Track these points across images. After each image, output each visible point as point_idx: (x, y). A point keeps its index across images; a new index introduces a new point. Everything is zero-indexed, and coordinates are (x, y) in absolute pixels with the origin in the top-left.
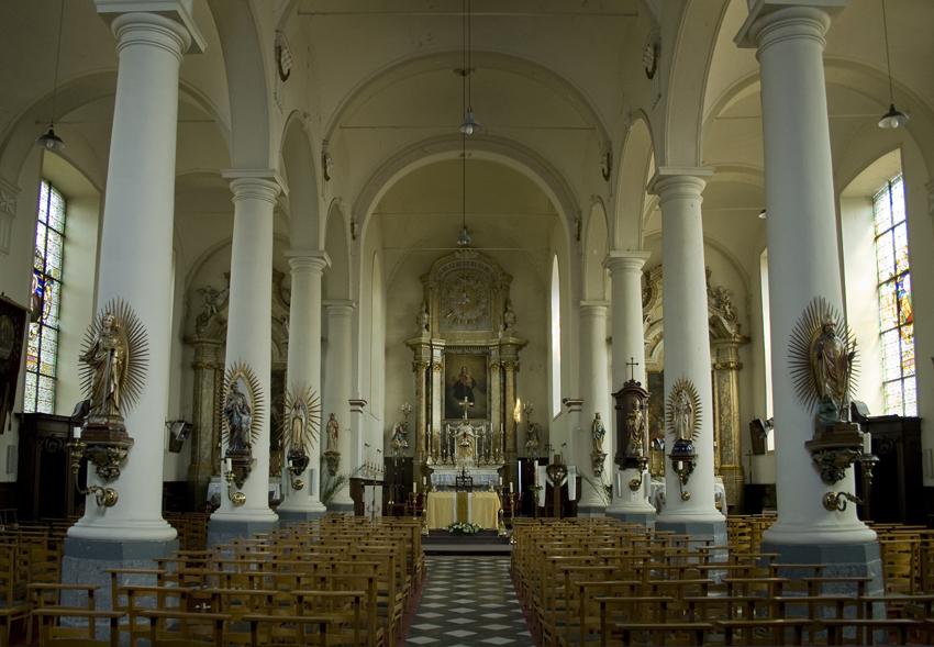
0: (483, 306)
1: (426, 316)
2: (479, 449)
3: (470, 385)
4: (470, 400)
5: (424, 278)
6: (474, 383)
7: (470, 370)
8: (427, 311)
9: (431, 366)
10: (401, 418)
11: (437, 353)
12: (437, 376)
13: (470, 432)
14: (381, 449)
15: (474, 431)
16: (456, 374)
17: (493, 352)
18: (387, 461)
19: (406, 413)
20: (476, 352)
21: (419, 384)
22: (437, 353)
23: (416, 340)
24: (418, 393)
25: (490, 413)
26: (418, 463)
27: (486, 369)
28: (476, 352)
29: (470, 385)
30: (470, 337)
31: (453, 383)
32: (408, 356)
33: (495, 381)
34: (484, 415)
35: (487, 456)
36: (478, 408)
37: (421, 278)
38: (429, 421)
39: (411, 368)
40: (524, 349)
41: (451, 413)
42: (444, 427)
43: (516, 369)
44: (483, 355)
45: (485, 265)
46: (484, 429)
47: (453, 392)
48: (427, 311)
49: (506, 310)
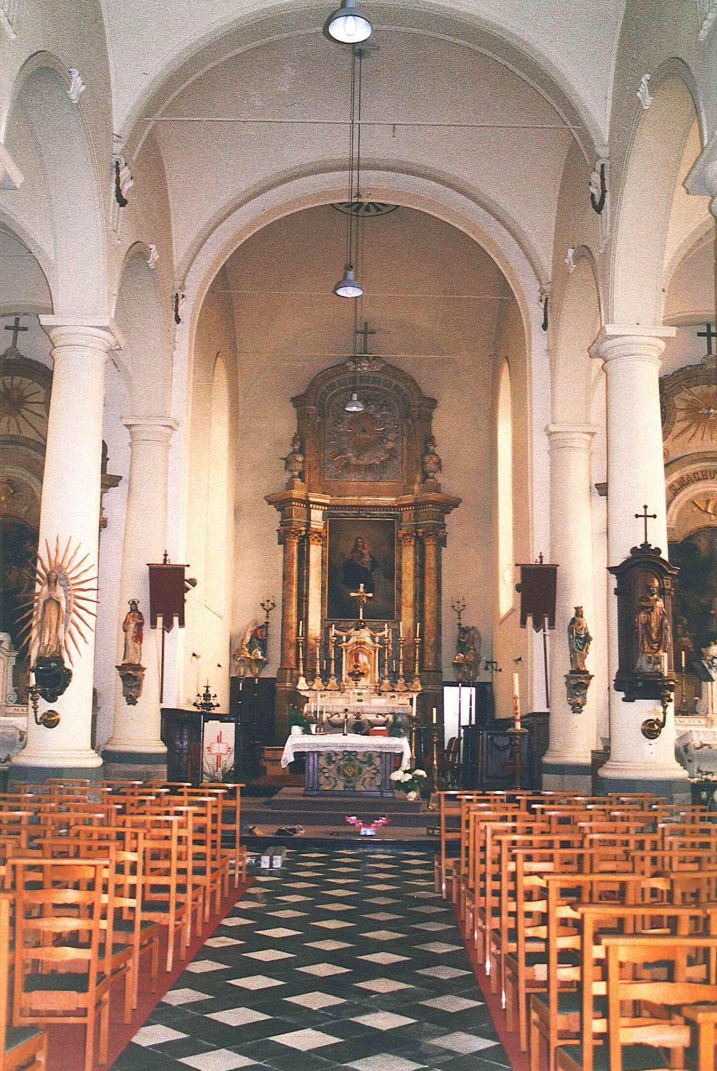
0: (390, 445)
2: (381, 666)
3: (368, 567)
5: (297, 401)
6: (374, 563)
8: (301, 451)
9: (307, 536)
11: (317, 515)
12: (316, 552)
13: (368, 640)
14: (225, 663)
15: (373, 638)
17: (406, 516)
18: (234, 682)
22: (317, 515)
25: (399, 610)
29: (368, 567)
33: (408, 558)
34: (391, 614)
37: (293, 400)
41: (339, 609)
42: (326, 629)
45: (394, 382)
49: (427, 452)
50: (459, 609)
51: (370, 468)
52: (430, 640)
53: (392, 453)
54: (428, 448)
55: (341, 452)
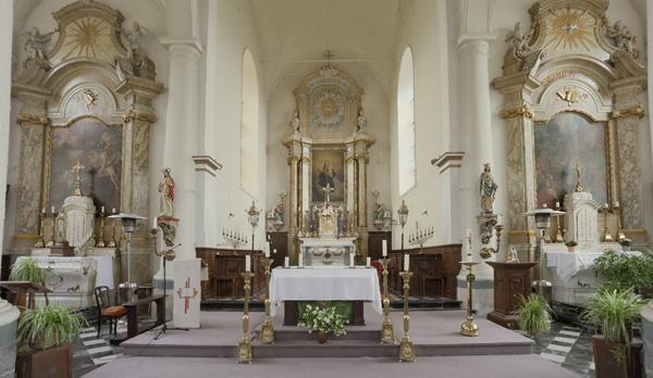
1: (297, 120)
2: (339, 225)
4: (332, 186)
6: (334, 174)
7: (330, 163)
8: (298, 117)
9: (301, 160)
10: (279, 201)
12: (306, 168)
16: (320, 167)
19: (283, 197)
20: (335, 148)
21: (291, 174)
22: (306, 150)
23: (289, 139)
24: (291, 182)
26: (291, 236)
27: (343, 162)
28: (335, 148)
30: (327, 137)
31: (318, 174)
32: (283, 150)
33: (350, 169)
34: (342, 199)
35: (345, 230)
36: (337, 194)
38: (299, 204)
39: (286, 163)
40: (372, 147)
41: (317, 197)
42: (311, 207)
43: (367, 162)
44: (340, 151)
46: (341, 208)
47: (318, 180)
48: (298, 117)
50: (376, 195)
51: (331, 125)
52: (361, 211)
53: (342, 117)
54: (359, 115)
55: (317, 118)
